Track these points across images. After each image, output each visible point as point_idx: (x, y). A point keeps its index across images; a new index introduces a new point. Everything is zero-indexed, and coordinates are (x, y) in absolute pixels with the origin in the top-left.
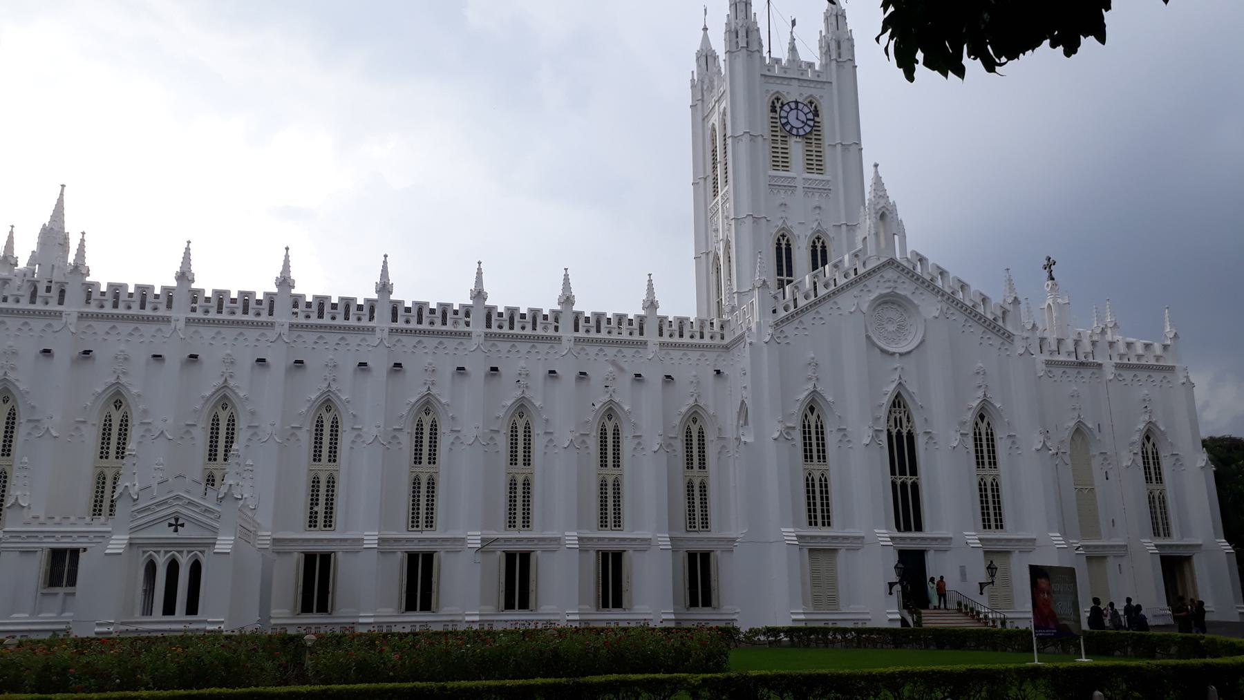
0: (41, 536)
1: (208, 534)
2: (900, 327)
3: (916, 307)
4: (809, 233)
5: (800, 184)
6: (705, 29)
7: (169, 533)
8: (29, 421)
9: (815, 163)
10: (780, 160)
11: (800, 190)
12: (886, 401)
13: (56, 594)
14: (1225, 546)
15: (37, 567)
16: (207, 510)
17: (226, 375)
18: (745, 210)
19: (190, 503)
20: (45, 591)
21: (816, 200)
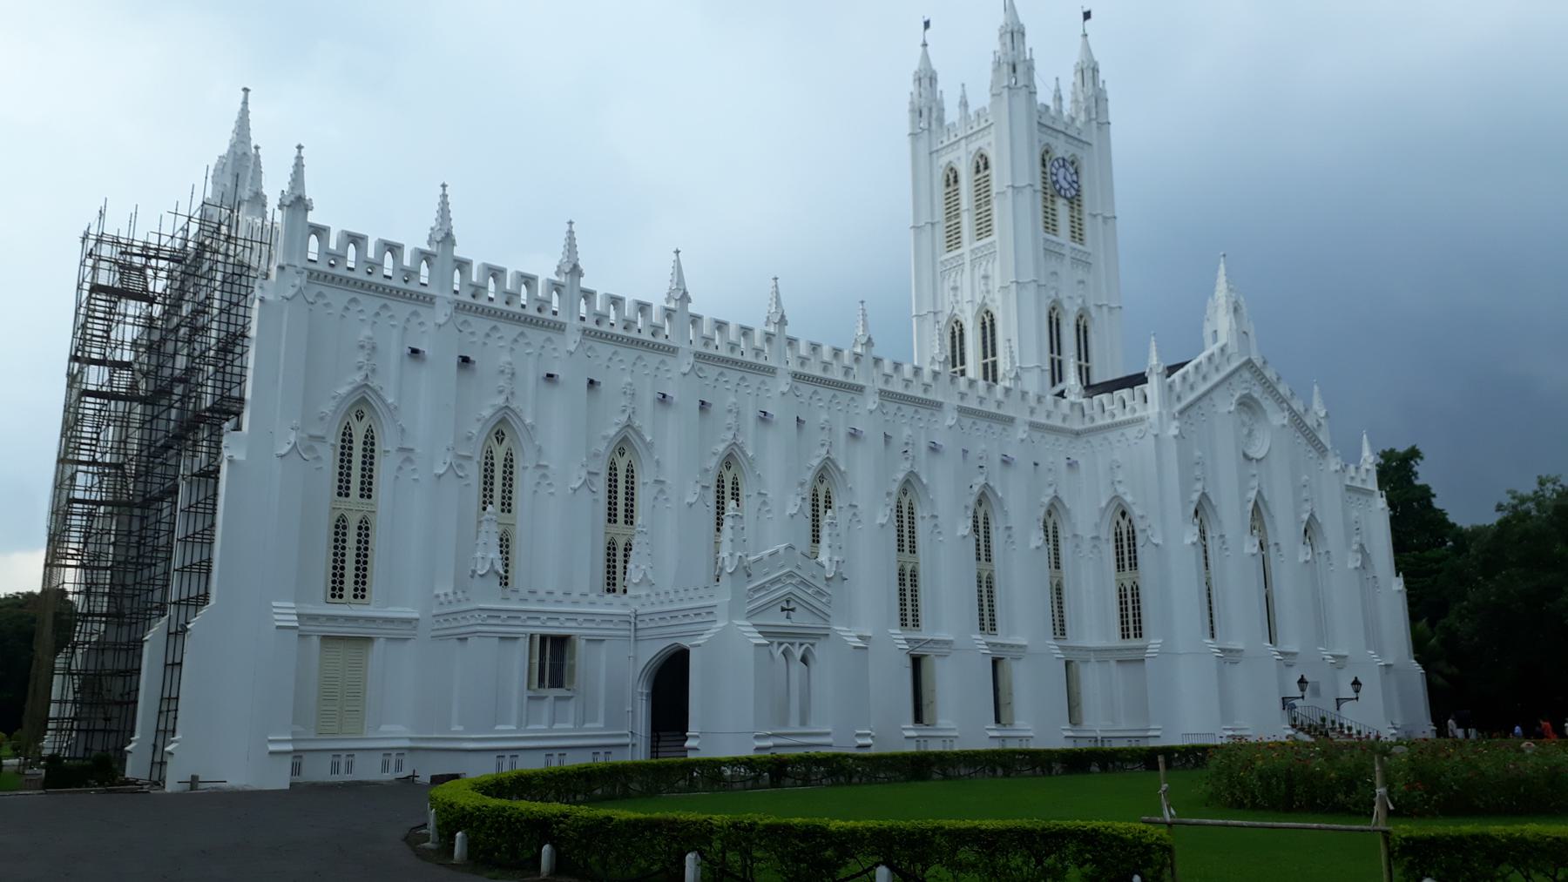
0: (524, 617)
1: (820, 623)
2: (1250, 434)
3: (1264, 412)
4: (1076, 309)
5: (1066, 251)
6: (925, 45)
7: (780, 620)
8: (401, 449)
9: (1077, 234)
10: (1050, 225)
11: (1067, 261)
12: (1250, 506)
13: (544, 698)
14: (1418, 669)
15: (519, 660)
16: (820, 593)
17: (629, 411)
18: (1028, 275)
19: (804, 582)
20: (531, 694)
21: (1080, 274)
